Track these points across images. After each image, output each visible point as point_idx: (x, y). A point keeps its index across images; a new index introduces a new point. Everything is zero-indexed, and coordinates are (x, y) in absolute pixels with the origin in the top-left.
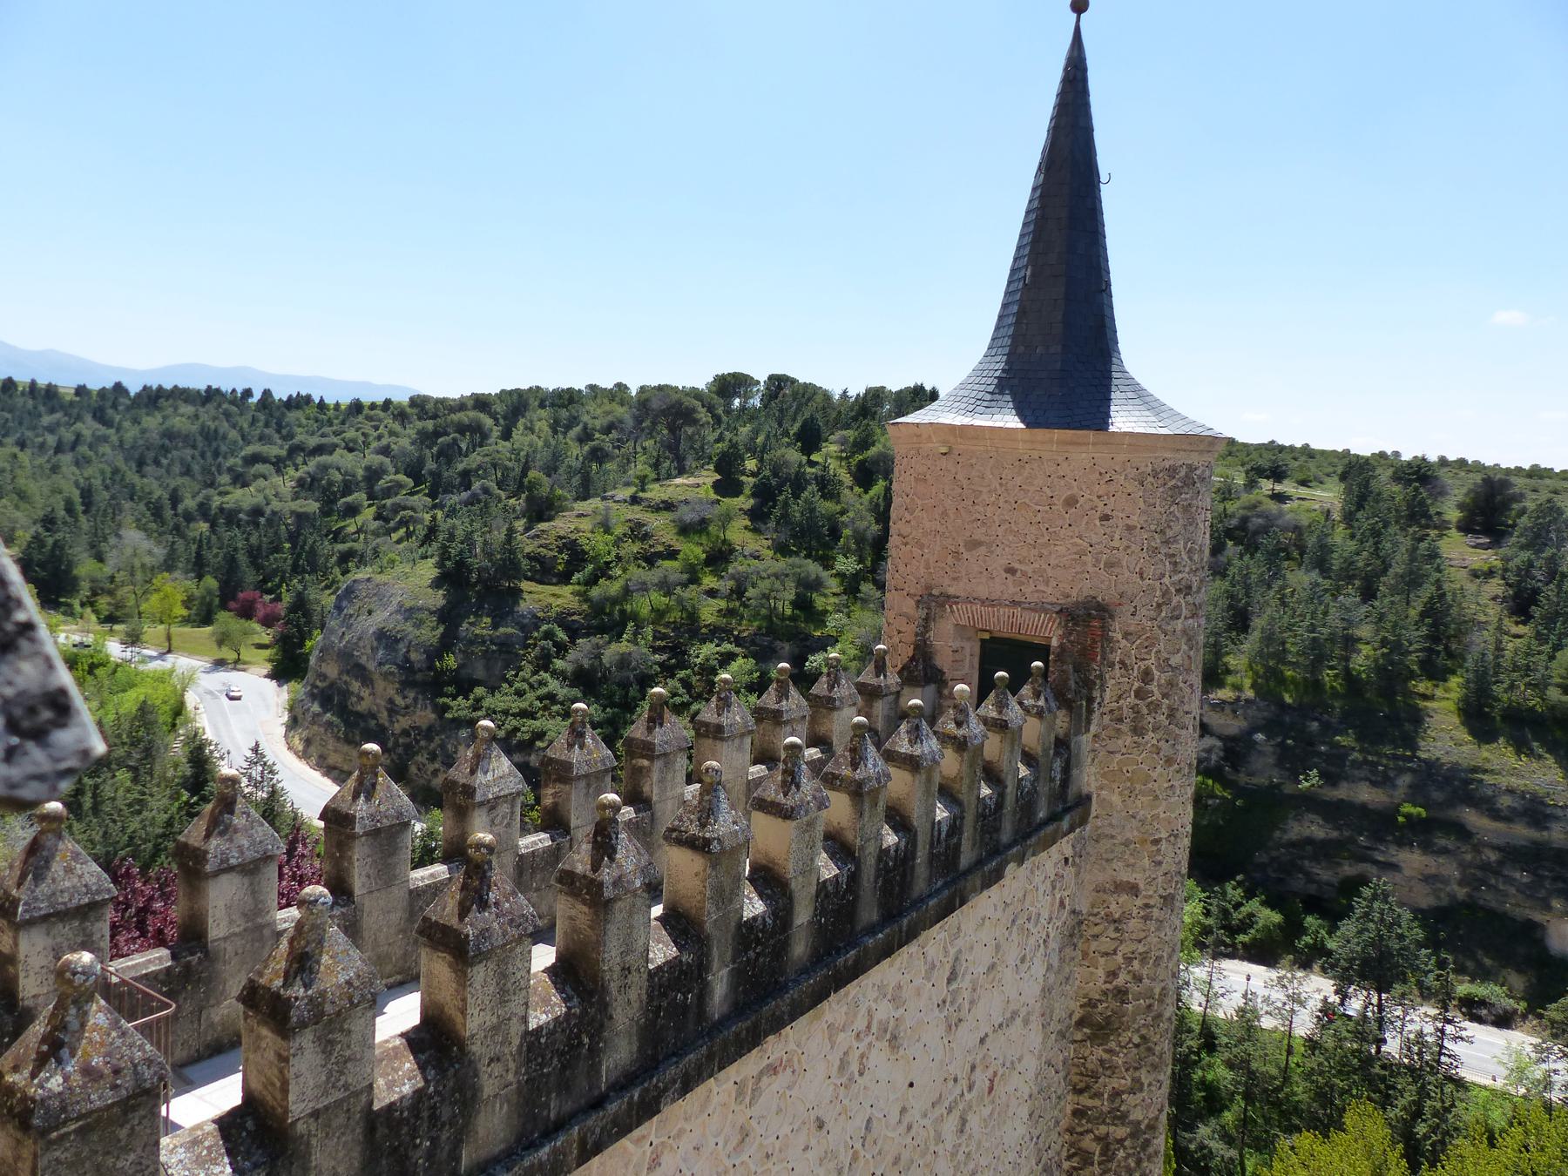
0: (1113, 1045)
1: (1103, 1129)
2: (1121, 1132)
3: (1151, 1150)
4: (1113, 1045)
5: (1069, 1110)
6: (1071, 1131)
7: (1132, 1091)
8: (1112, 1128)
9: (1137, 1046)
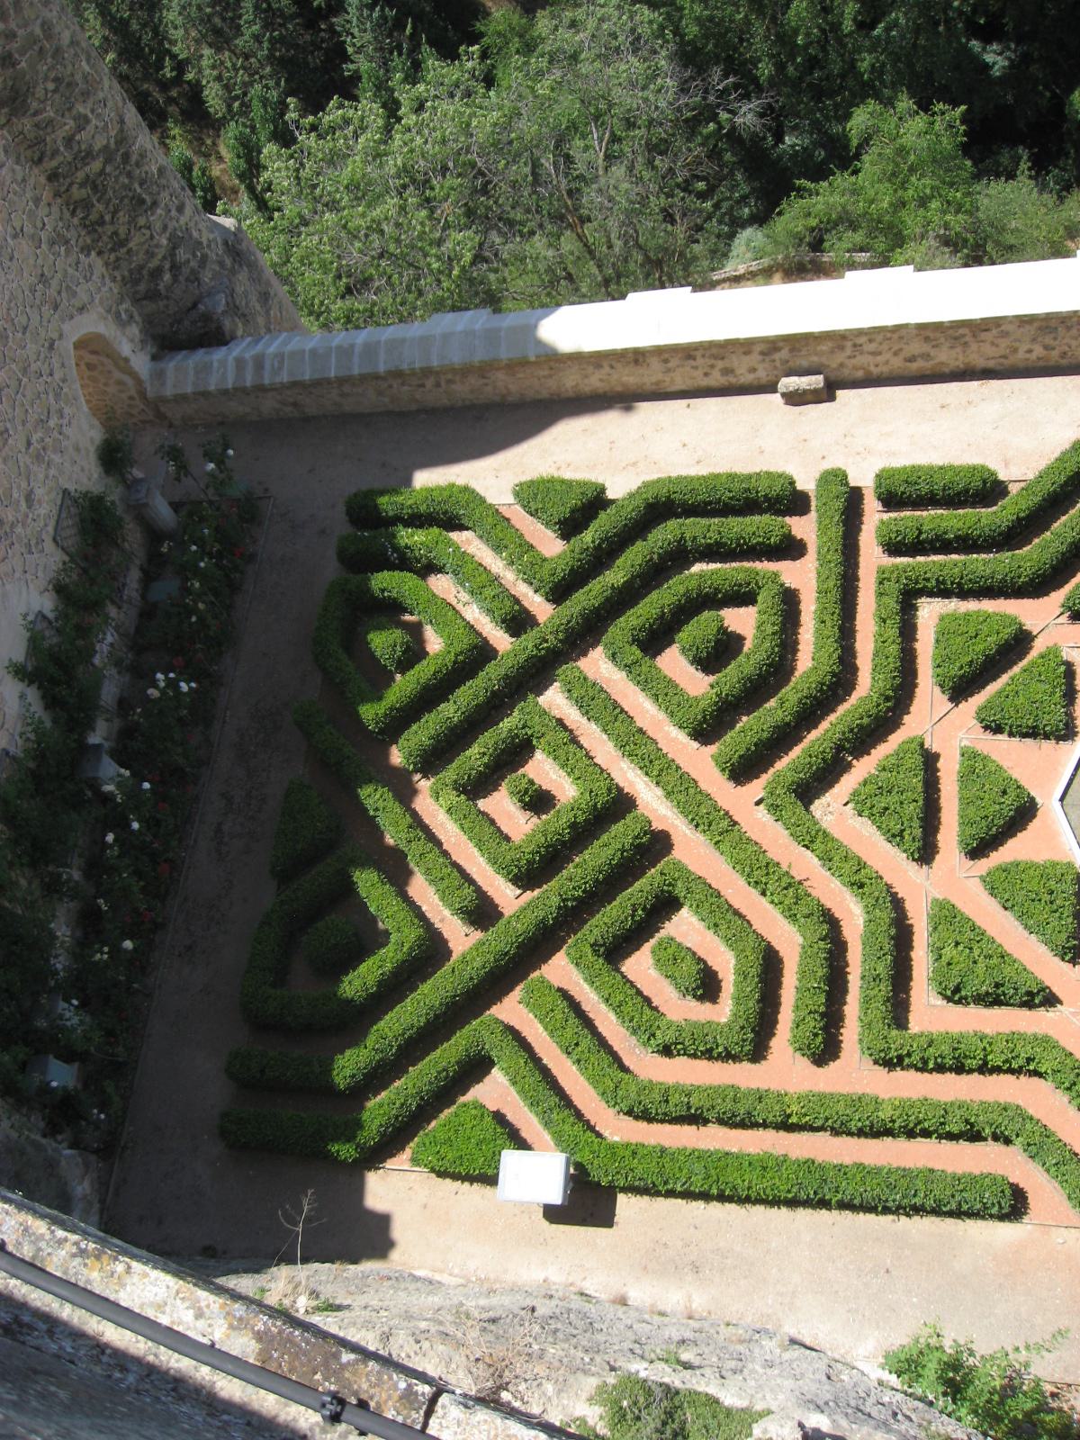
0: (35, 105)
1: (80, 175)
2: (96, 166)
3: (134, 158)
4: (35, 105)
5: (43, 180)
6: (57, 194)
7: (80, 129)
8: (87, 169)
9: (55, 91)
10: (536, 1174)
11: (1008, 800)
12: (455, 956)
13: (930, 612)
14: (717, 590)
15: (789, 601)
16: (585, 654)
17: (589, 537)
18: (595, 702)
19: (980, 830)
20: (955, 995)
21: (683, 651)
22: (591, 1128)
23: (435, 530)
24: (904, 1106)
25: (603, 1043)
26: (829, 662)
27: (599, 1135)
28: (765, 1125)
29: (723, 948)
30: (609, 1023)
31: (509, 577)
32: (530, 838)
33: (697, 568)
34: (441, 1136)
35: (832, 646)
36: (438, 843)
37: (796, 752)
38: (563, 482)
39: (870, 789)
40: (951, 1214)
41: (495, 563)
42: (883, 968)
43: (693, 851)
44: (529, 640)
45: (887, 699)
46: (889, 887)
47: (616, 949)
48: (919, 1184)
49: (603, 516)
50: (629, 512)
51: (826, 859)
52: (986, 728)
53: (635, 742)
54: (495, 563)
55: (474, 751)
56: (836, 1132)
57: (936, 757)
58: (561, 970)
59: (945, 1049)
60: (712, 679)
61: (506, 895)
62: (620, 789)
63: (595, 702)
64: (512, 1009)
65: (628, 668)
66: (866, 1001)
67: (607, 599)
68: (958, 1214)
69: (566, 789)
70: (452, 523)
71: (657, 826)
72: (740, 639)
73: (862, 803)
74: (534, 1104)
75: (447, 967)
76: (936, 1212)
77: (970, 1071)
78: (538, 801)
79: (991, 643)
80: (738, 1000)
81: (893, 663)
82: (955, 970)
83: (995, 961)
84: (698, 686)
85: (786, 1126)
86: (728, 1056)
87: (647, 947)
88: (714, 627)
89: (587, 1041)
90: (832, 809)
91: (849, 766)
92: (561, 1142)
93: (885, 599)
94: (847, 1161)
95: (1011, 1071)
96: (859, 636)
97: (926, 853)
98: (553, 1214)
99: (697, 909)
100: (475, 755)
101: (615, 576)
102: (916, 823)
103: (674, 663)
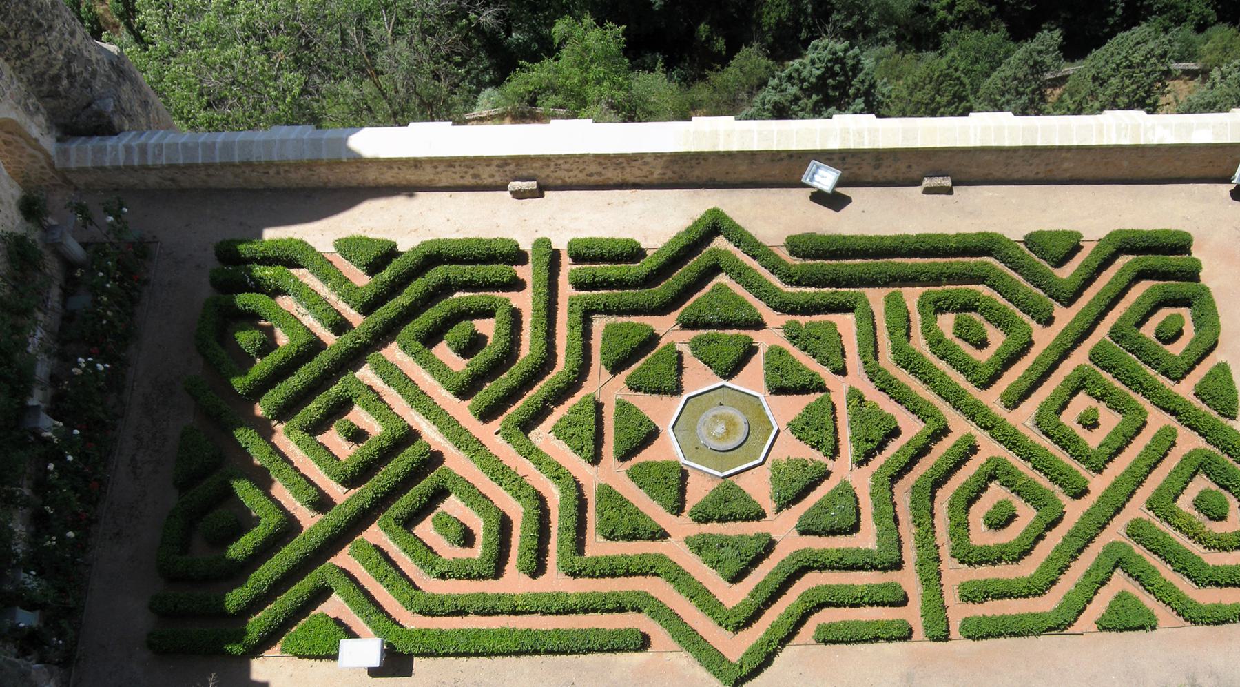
10: (363, 651)
11: (642, 428)
12: (304, 530)
13: (599, 323)
14: (470, 309)
15: (516, 315)
16: (385, 346)
17: (386, 274)
18: (392, 375)
19: (626, 445)
20: (611, 536)
21: (449, 345)
22: (397, 623)
23: (280, 268)
24: (582, 596)
25: (403, 575)
26: (540, 351)
27: (401, 626)
28: (502, 613)
29: (476, 516)
30: (406, 563)
31: (333, 298)
32: (352, 458)
33: (457, 295)
34: (300, 635)
35: (541, 343)
36: (291, 463)
37: (520, 403)
38: (368, 239)
39: (564, 423)
40: (608, 651)
41: (324, 290)
42: (571, 523)
43: (457, 462)
44: (348, 338)
45: (574, 372)
46: (575, 478)
47: (410, 521)
48: (591, 637)
49: (395, 262)
50: (413, 260)
51: (538, 464)
52: (631, 389)
53: (419, 399)
54: (324, 290)
55: (313, 406)
56: (543, 613)
57: (602, 405)
58: (375, 534)
59: (605, 565)
60: (467, 361)
61: (338, 492)
62: (410, 427)
63: (392, 375)
64: (344, 558)
65: (414, 355)
66: (561, 542)
67: (399, 313)
68: (612, 651)
69: (375, 428)
70: (292, 263)
71: (434, 448)
72: (485, 338)
73: (560, 432)
74: (360, 612)
75: (300, 536)
76: (601, 651)
77: (619, 576)
78: (357, 436)
79: (636, 340)
80: (485, 545)
81: (578, 352)
82: (611, 522)
83: (634, 516)
84: (460, 366)
85: (514, 612)
86: (480, 577)
87: (429, 518)
88: (468, 331)
89: (392, 574)
90: (542, 436)
91: (551, 412)
92: (377, 632)
93: (574, 315)
94: (550, 628)
95: (642, 574)
96: (557, 337)
97: (596, 459)
98: (373, 672)
99: (460, 495)
100: (314, 408)
101: (404, 299)
102: (591, 442)
103: (443, 351)
